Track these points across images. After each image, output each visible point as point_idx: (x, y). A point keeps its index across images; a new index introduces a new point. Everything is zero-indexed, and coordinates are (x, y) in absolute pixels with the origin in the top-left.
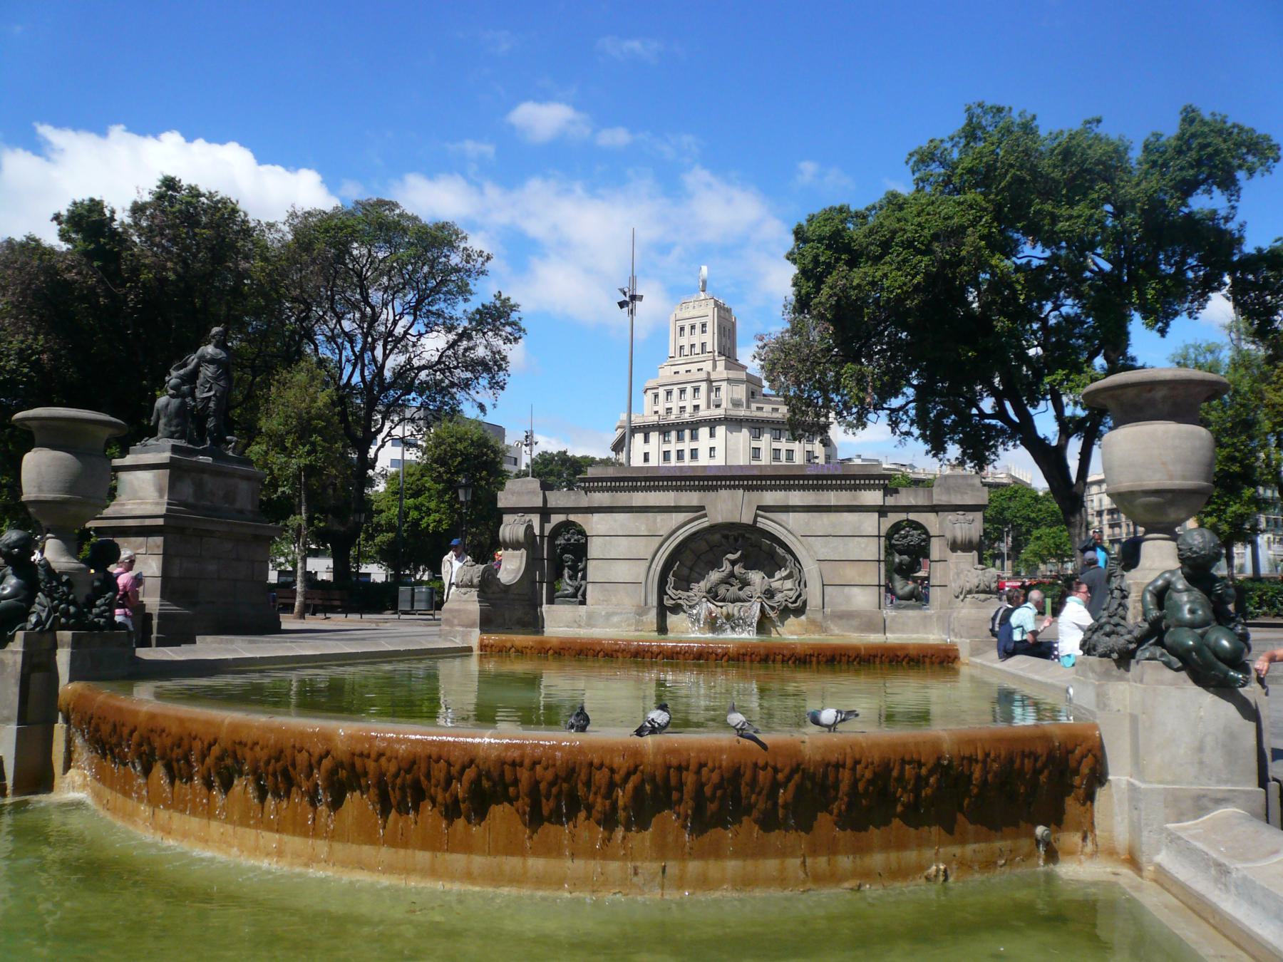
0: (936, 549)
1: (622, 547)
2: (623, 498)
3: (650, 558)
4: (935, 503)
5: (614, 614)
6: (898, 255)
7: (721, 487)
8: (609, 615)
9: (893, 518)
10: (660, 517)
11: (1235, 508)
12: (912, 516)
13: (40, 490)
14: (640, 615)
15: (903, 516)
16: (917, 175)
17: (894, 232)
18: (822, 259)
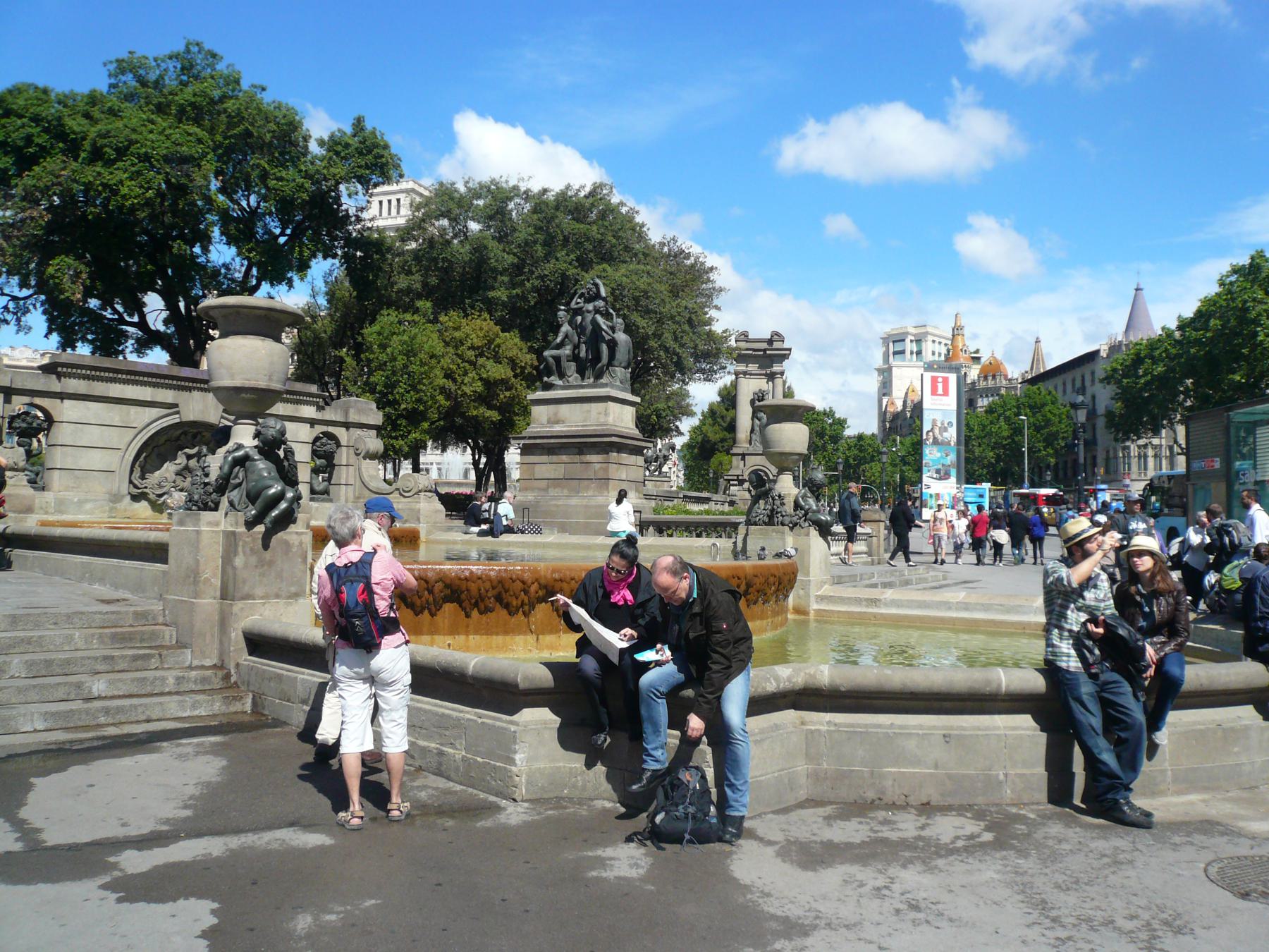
0: (343, 456)
1: (93, 435)
2: (100, 388)
3: (123, 447)
4: (351, 420)
5: (87, 501)
6: (133, 165)
7: (194, 388)
8: (81, 503)
9: (319, 429)
10: (134, 410)
11: (415, 435)
12: (331, 429)
13: (270, 379)
14: (114, 502)
15: (324, 428)
16: (113, 81)
17: (132, 142)
18: (37, 140)
